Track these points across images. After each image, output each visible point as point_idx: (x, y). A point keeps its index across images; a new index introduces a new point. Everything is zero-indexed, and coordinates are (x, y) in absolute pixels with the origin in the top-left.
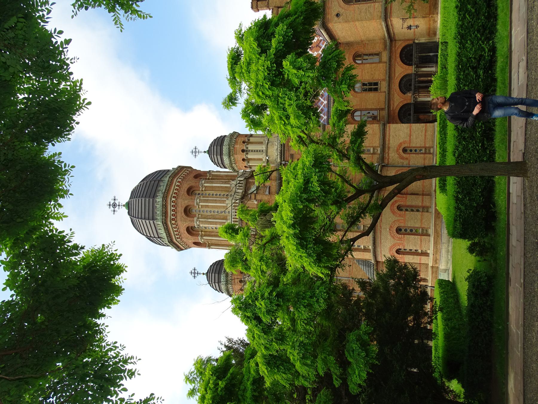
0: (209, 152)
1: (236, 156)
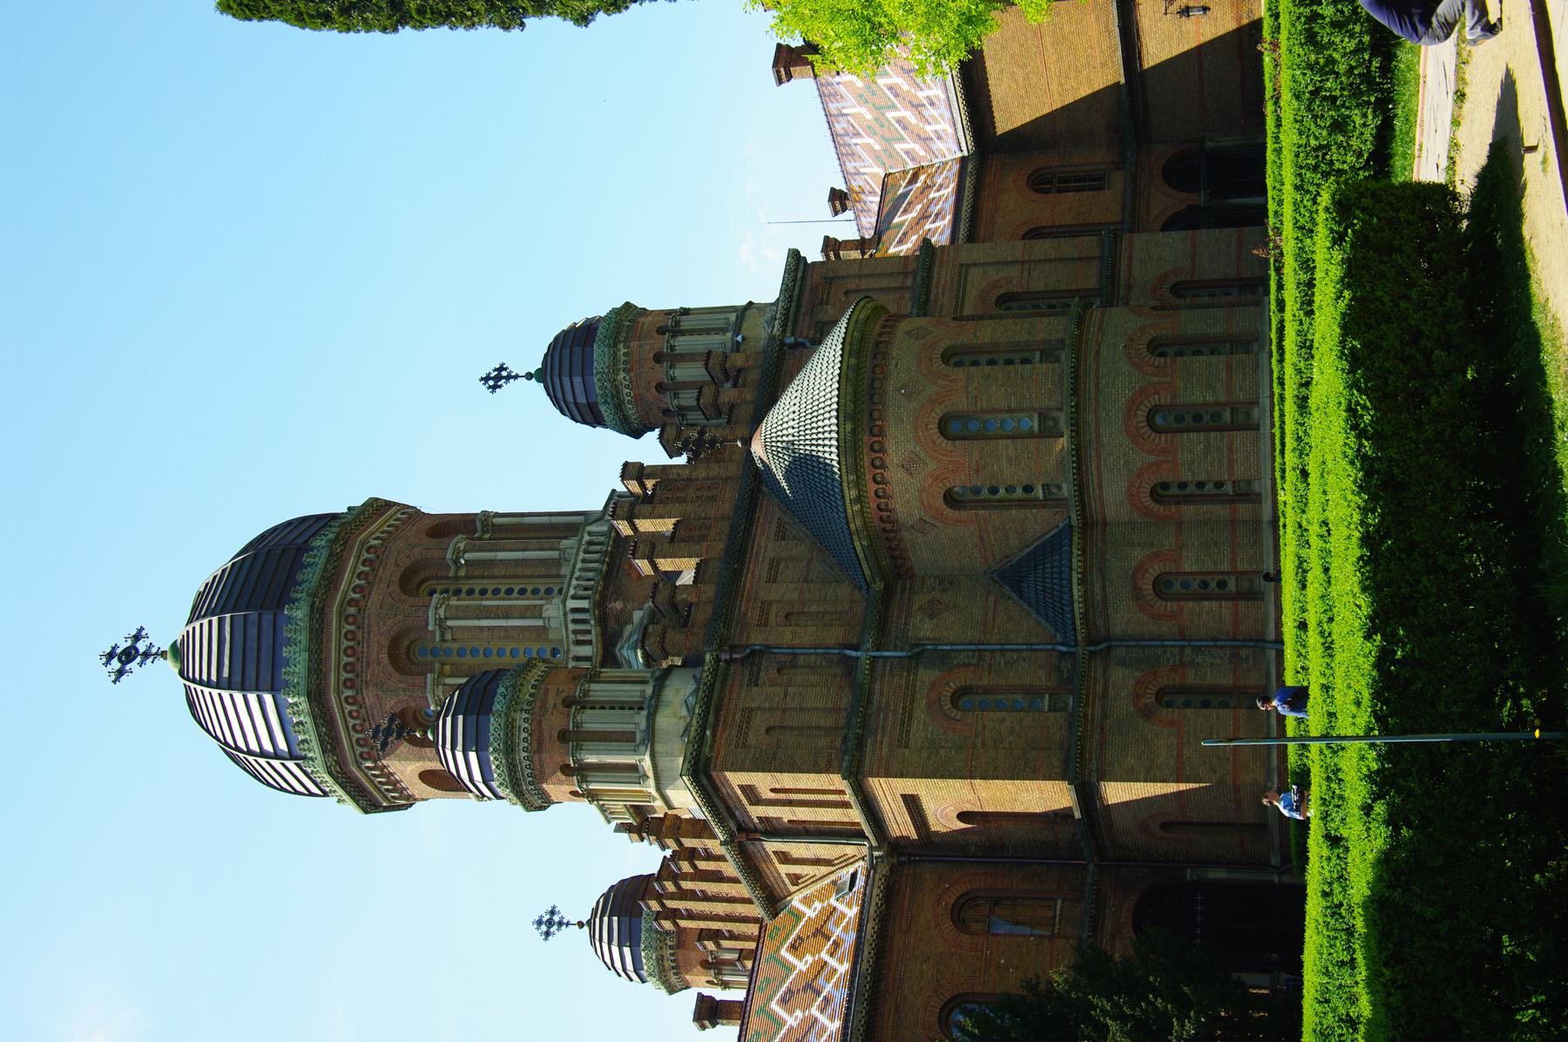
0: (540, 375)
1: (634, 344)
